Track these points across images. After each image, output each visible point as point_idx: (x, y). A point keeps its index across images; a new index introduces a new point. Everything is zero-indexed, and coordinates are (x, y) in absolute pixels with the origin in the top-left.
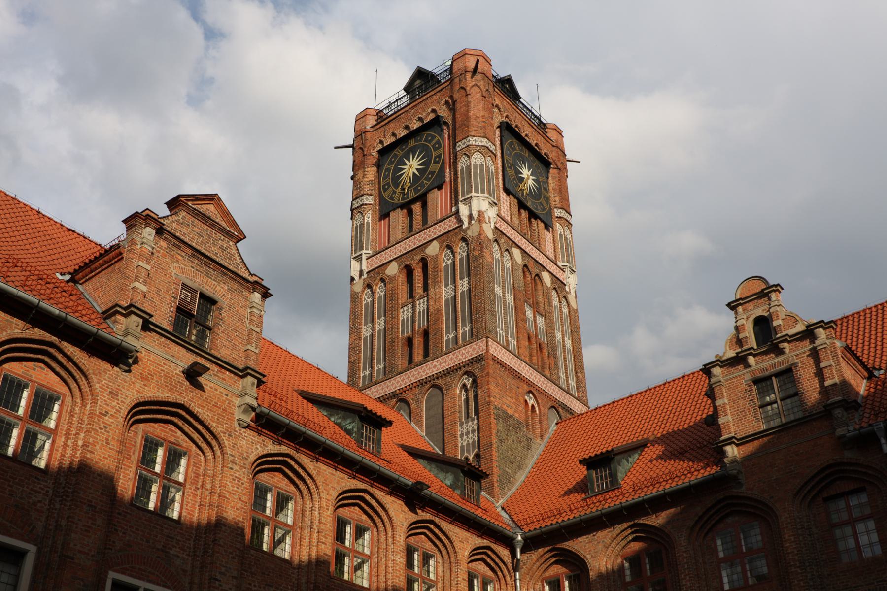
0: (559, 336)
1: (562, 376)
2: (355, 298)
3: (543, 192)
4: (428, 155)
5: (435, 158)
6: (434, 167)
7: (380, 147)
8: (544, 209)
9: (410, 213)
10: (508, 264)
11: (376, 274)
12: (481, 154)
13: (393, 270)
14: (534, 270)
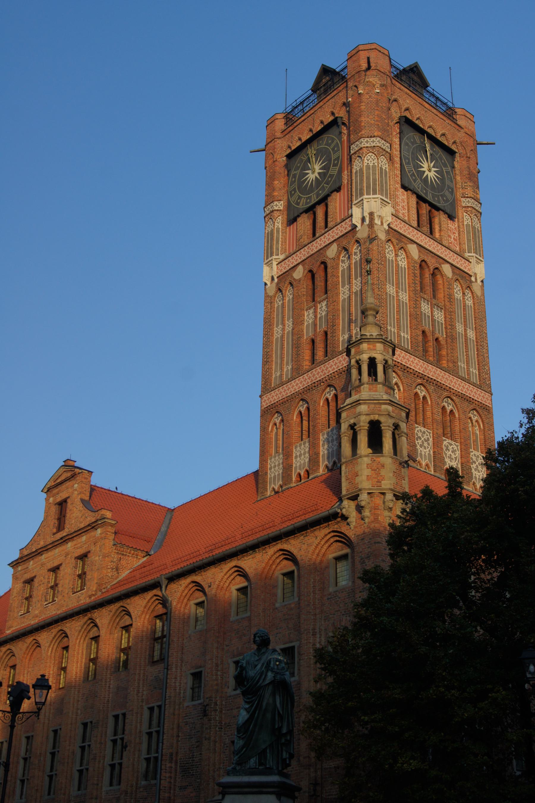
0: (460, 328)
1: (462, 365)
2: (269, 300)
3: (447, 182)
5: (335, 160)
6: (333, 171)
7: (289, 151)
8: (447, 201)
10: (403, 263)
11: (284, 279)
12: (374, 156)
13: (299, 274)
14: (432, 263)
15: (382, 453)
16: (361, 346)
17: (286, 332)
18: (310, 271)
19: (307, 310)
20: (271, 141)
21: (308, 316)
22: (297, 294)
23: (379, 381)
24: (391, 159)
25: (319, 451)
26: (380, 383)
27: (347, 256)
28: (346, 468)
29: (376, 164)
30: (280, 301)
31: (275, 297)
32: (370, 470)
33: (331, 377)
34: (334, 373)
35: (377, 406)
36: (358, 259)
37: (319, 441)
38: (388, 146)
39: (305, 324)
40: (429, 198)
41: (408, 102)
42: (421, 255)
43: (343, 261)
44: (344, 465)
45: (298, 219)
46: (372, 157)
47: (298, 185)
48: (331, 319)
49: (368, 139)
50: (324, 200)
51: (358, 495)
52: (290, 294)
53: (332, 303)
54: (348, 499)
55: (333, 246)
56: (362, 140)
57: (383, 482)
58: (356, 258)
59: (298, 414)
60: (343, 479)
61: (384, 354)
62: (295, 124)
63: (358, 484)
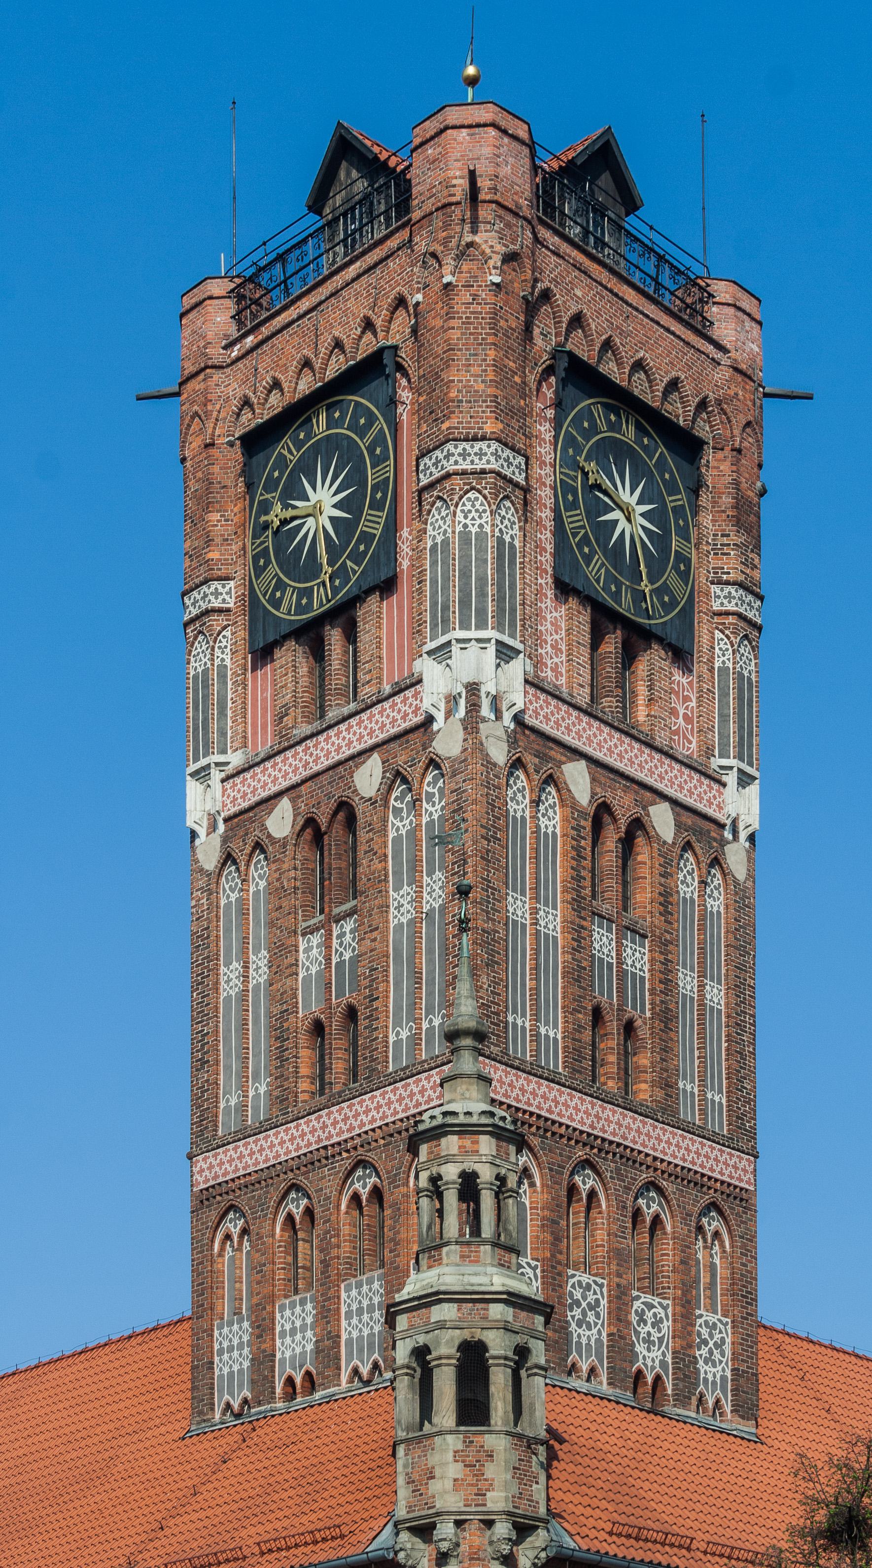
4: (357, 478)
9: (318, 652)
15: (489, 1425)
16: (443, 1141)
17: (251, 986)
18: (311, 822)
19: (304, 935)
20: (197, 373)
21: (307, 951)
22: (278, 884)
23: (483, 1236)
24: (526, 508)
25: (339, 1331)
26: (485, 1242)
27: (408, 798)
28: (406, 1455)
29: (488, 529)
30: (232, 890)
31: (220, 875)
32: (461, 1465)
33: (366, 1140)
34: (373, 1130)
35: (479, 1306)
36: (436, 816)
37: (339, 1303)
38: (518, 467)
39: (301, 976)
40: (625, 606)
41: (579, 293)
42: (598, 790)
43: (397, 812)
44: (403, 1446)
45: (278, 653)
46: (478, 504)
47: (277, 547)
48: (369, 970)
49: (466, 445)
50: (344, 614)
51: (433, 1526)
52: (261, 877)
53: (372, 929)
54: (410, 1529)
55: (369, 762)
56: (450, 446)
57: (489, 1494)
58: (433, 810)
59: (284, 1224)
60: (401, 1480)
61: (498, 1162)
62: (265, 331)
63: (434, 1497)
